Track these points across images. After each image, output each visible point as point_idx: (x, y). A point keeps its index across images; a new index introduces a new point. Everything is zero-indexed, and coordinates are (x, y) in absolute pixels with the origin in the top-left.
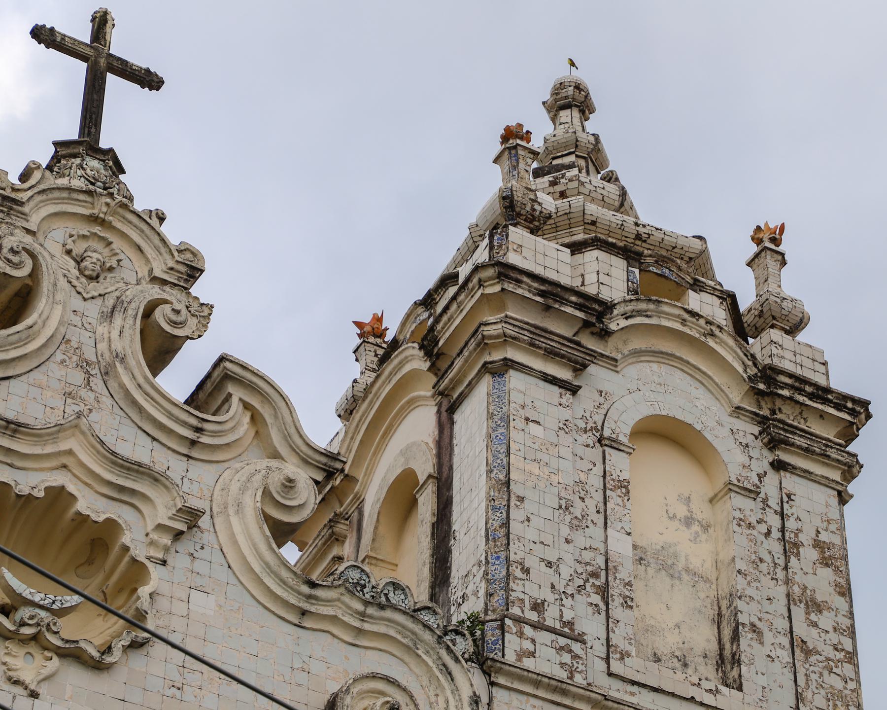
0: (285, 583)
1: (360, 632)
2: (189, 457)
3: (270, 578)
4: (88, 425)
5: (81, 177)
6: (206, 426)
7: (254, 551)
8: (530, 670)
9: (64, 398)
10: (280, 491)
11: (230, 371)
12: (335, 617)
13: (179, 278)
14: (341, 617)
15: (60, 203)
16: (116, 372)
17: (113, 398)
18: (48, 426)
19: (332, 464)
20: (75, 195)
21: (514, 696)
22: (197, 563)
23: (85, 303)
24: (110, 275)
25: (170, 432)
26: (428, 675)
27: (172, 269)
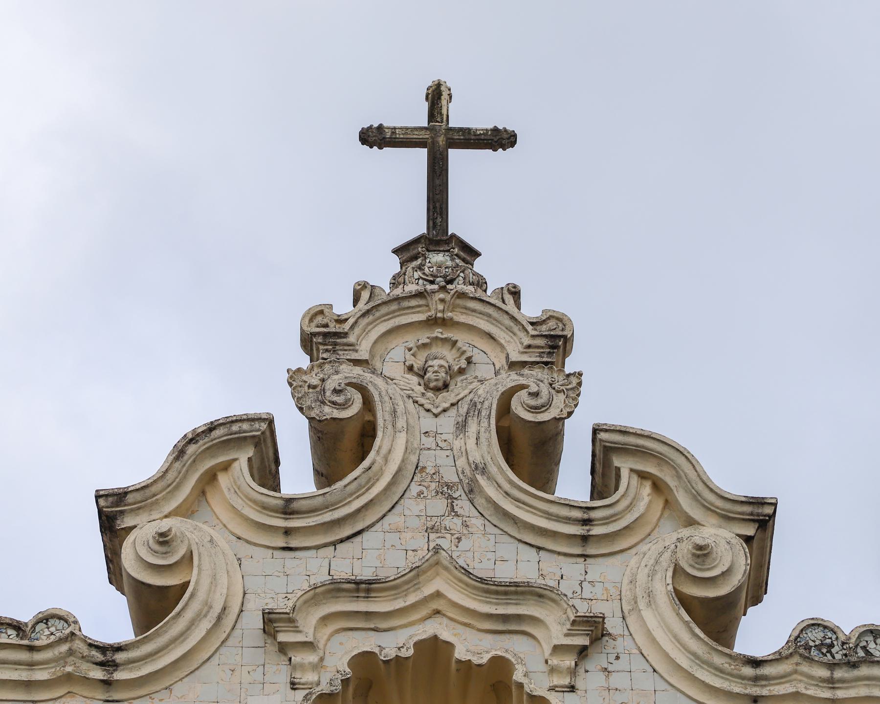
0: (721, 671)
2: (585, 556)
3: (703, 671)
4: (449, 558)
5: (419, 279)
6: (594, 515)
7: (677, 644)
9: (427, 534)
10: (693, 564)
11: (609, 442)
13: (541, 355)
14: (804, 691)
15: (391, 318)
16: (480, 486)
17: (484, 517)
18: (402, 574)
19: (760, 511)
20: (406, 304)
23: (437, 419)
24: (459, 379)
27: (529, 347)
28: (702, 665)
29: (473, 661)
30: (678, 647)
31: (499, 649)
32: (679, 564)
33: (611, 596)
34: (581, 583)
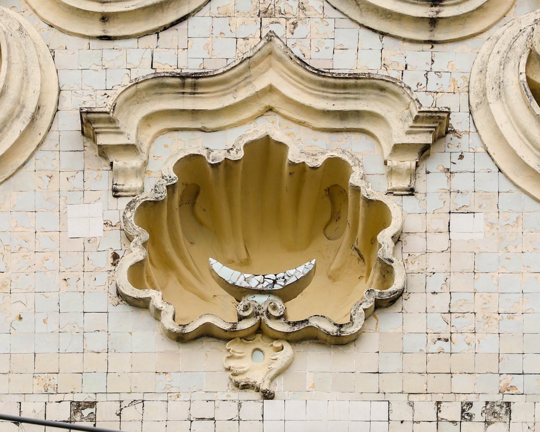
22: (456, 178)
29: (307, 164)
31: (335, 150)
32: (535, 49)
33: (458, 87)
34: (427, 74)
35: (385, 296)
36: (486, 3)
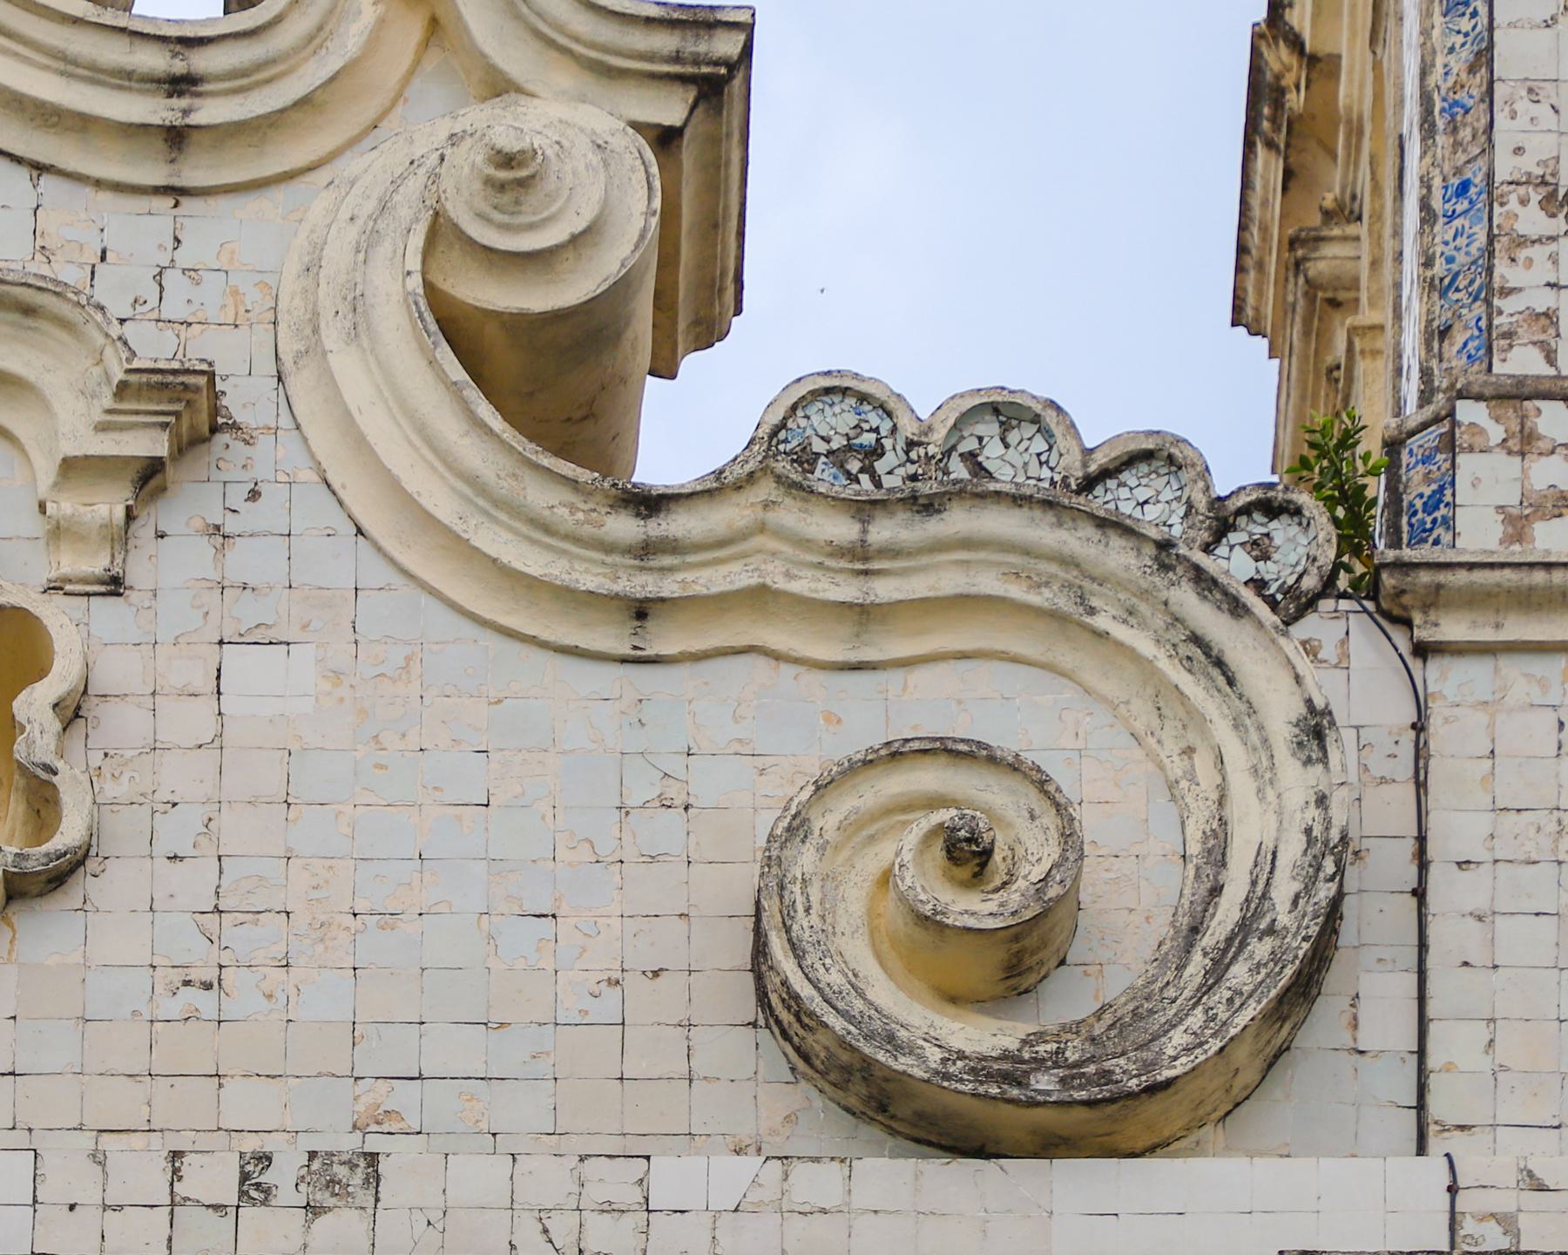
0: (547, 529)
1: (864, 614)
2: (177, 193)
3: (497, 529)
6: (203, 61)
8: (1553, 559)
12: (763, 588)
14: (782, 584)
21: (1513, 669)
25: (81, 124)
26: (1150, 691)
28: (494, 512)
30: (426, 461)
32: (446, 211)
33: (247, 311)
34: (160, 274)
35: (32, 866)
36: (319, 91)
